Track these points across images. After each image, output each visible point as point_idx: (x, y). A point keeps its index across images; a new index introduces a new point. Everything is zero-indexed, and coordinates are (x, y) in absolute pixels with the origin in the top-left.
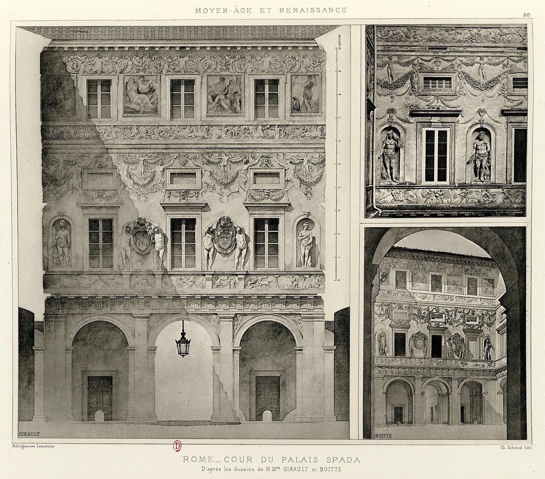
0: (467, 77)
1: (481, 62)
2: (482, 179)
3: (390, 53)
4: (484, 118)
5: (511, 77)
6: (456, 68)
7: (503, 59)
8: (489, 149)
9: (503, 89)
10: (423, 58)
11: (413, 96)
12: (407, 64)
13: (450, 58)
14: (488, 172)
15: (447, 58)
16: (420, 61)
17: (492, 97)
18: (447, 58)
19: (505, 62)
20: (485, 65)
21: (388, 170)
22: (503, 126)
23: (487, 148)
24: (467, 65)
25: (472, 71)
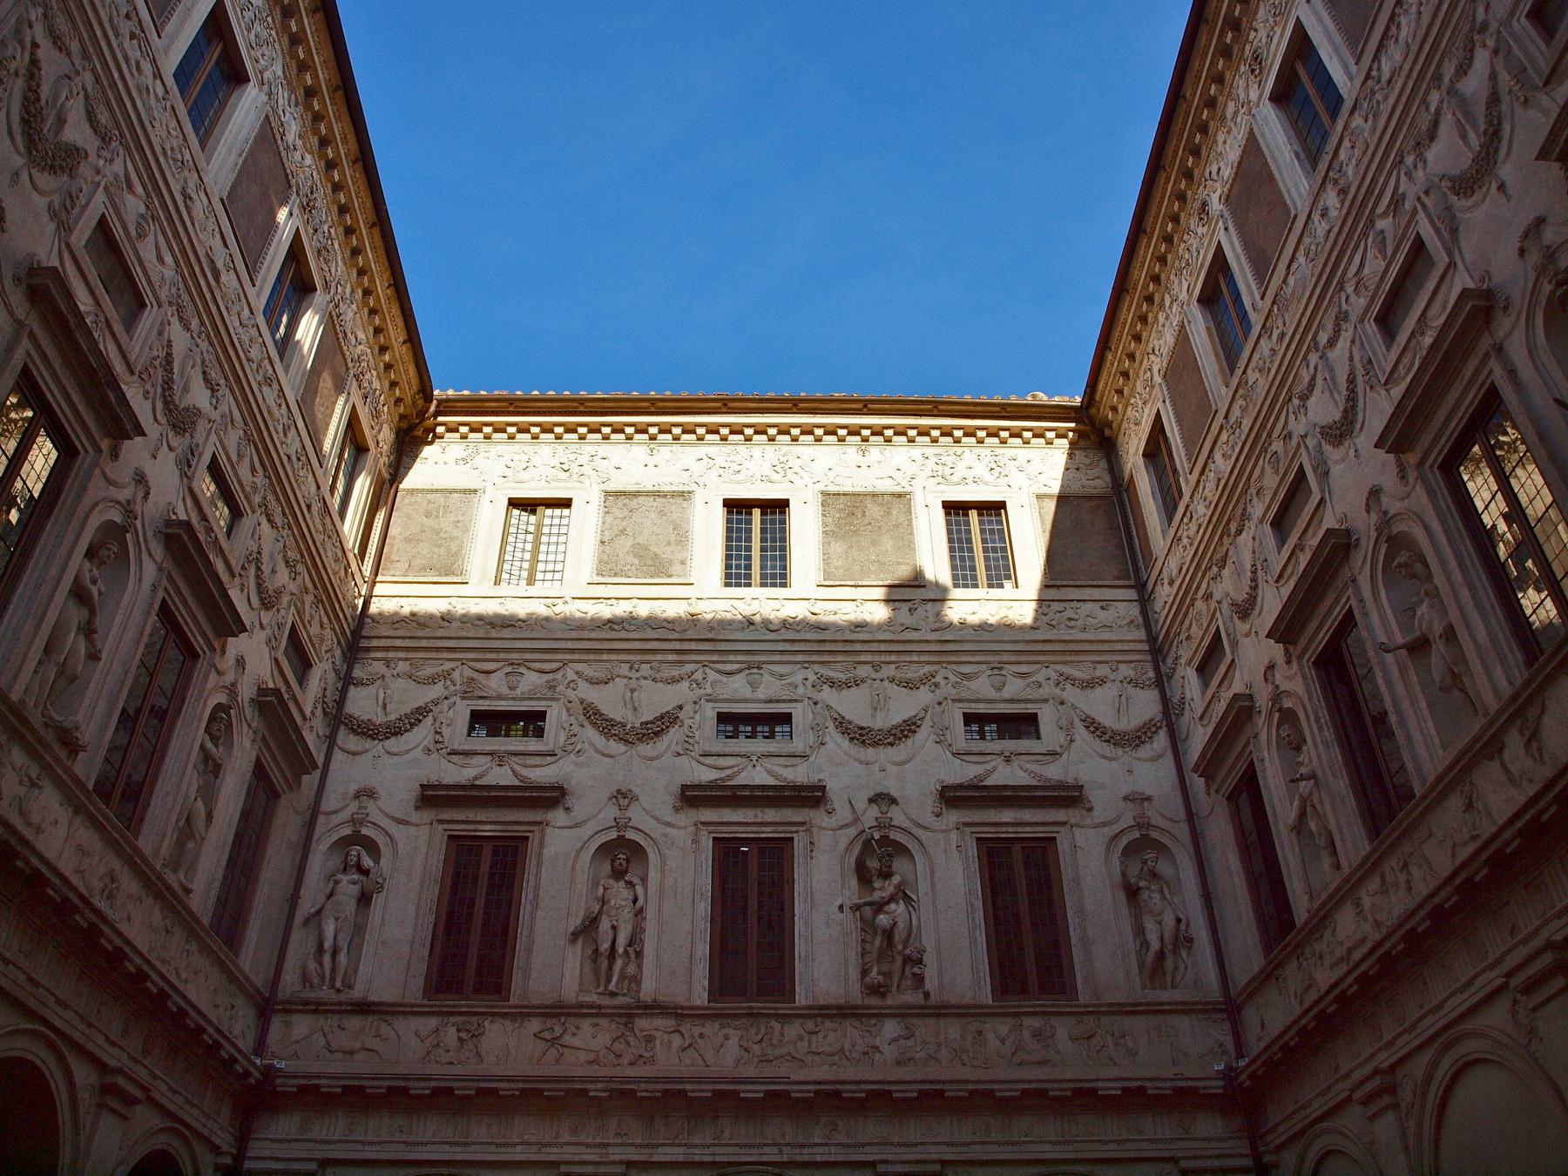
0: (593, 715)
1: (634, 675)
2: (612, 987)
3: (391, 655)
4: (629, 814)
5: (710, 712)
6: (560, 688)
7: (691, 667)
8: (641, 902)
9: (688, 740)
10: (478, 665)
11: (435, 756)
12: (432, 680)
13: (546, 666)
14: (632, 969)
15: (537, 666)
16: (468, 673)
17: (652, 759)
18: (537, 666)
19: (698, 676)
20: (643, 682)
21: (327, 958)
22: (682, 837)
23: (635, 900)
24: (593, 682)
25: (608, 700)
